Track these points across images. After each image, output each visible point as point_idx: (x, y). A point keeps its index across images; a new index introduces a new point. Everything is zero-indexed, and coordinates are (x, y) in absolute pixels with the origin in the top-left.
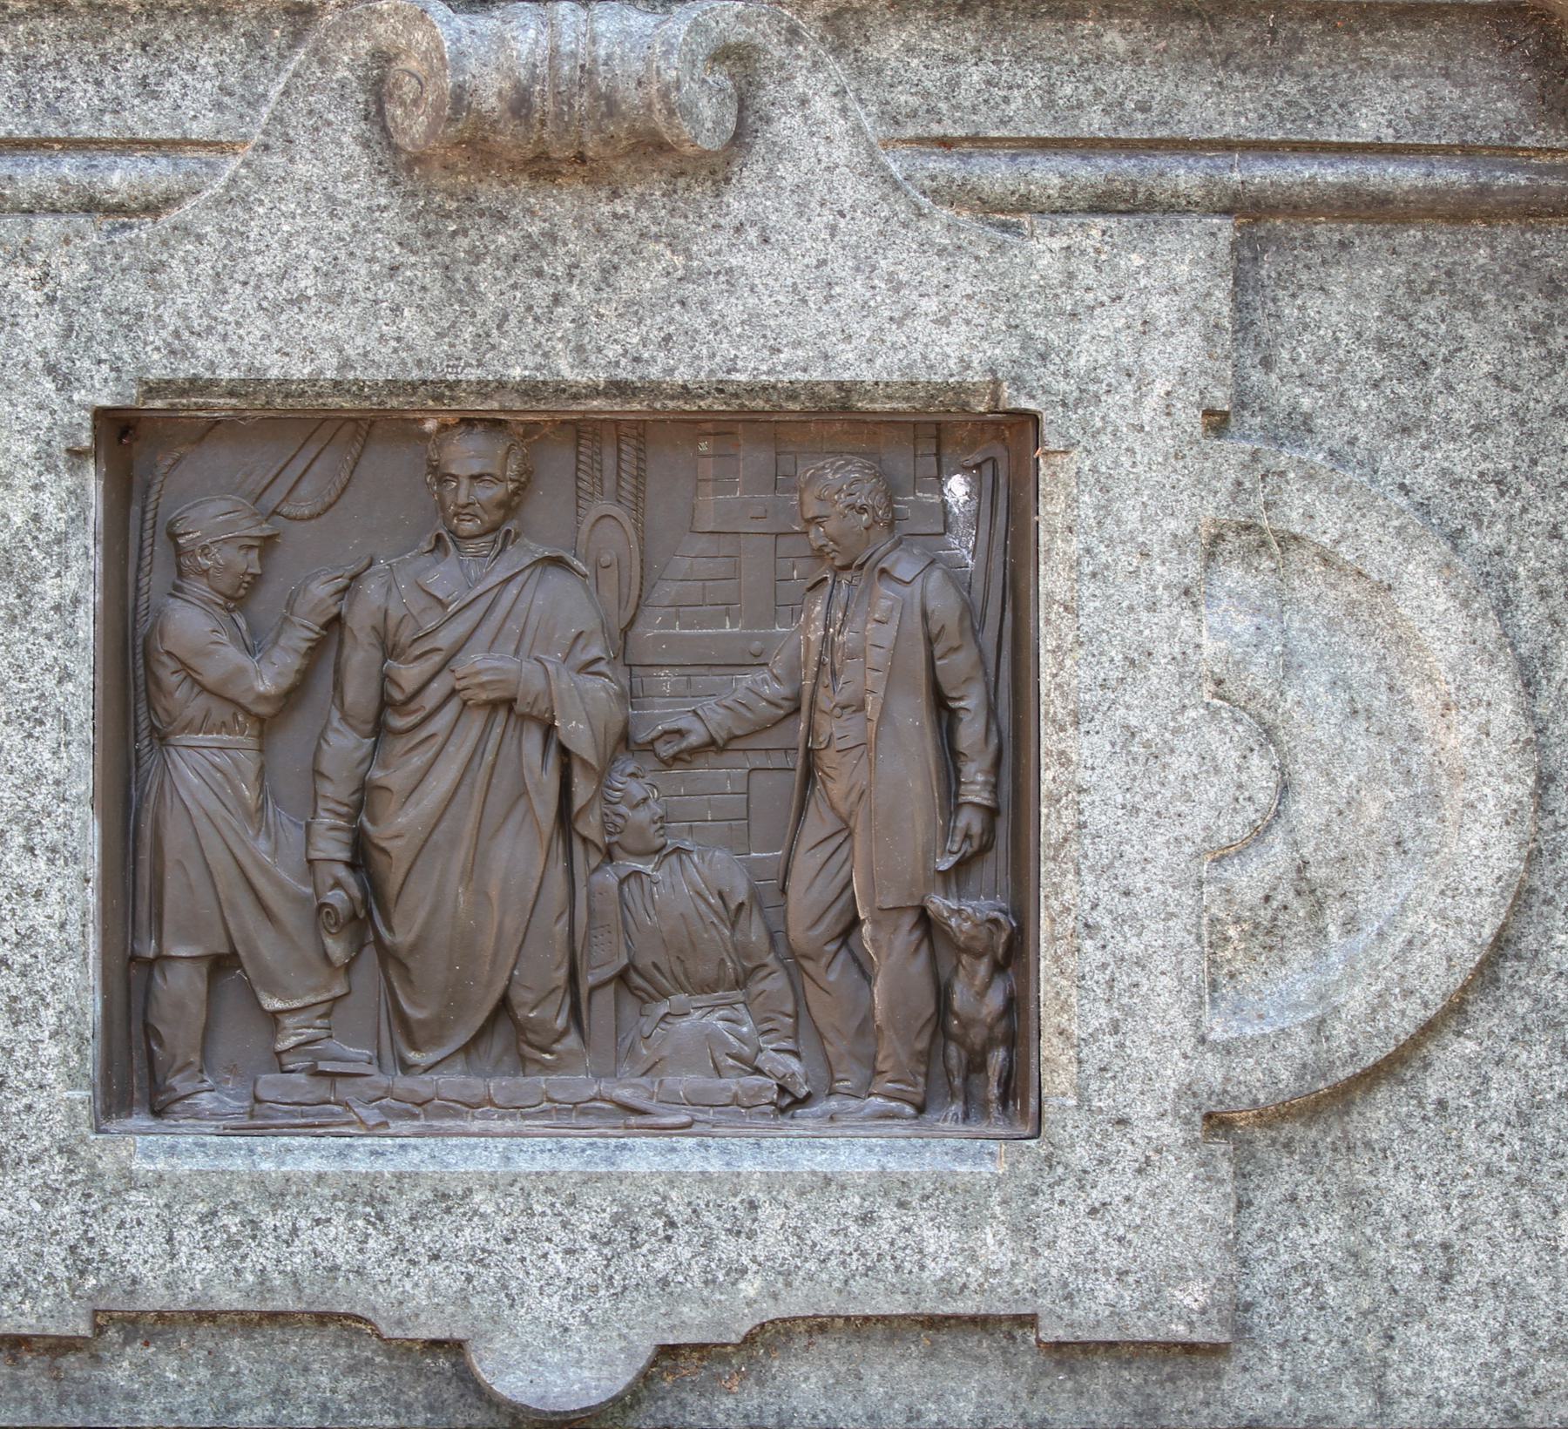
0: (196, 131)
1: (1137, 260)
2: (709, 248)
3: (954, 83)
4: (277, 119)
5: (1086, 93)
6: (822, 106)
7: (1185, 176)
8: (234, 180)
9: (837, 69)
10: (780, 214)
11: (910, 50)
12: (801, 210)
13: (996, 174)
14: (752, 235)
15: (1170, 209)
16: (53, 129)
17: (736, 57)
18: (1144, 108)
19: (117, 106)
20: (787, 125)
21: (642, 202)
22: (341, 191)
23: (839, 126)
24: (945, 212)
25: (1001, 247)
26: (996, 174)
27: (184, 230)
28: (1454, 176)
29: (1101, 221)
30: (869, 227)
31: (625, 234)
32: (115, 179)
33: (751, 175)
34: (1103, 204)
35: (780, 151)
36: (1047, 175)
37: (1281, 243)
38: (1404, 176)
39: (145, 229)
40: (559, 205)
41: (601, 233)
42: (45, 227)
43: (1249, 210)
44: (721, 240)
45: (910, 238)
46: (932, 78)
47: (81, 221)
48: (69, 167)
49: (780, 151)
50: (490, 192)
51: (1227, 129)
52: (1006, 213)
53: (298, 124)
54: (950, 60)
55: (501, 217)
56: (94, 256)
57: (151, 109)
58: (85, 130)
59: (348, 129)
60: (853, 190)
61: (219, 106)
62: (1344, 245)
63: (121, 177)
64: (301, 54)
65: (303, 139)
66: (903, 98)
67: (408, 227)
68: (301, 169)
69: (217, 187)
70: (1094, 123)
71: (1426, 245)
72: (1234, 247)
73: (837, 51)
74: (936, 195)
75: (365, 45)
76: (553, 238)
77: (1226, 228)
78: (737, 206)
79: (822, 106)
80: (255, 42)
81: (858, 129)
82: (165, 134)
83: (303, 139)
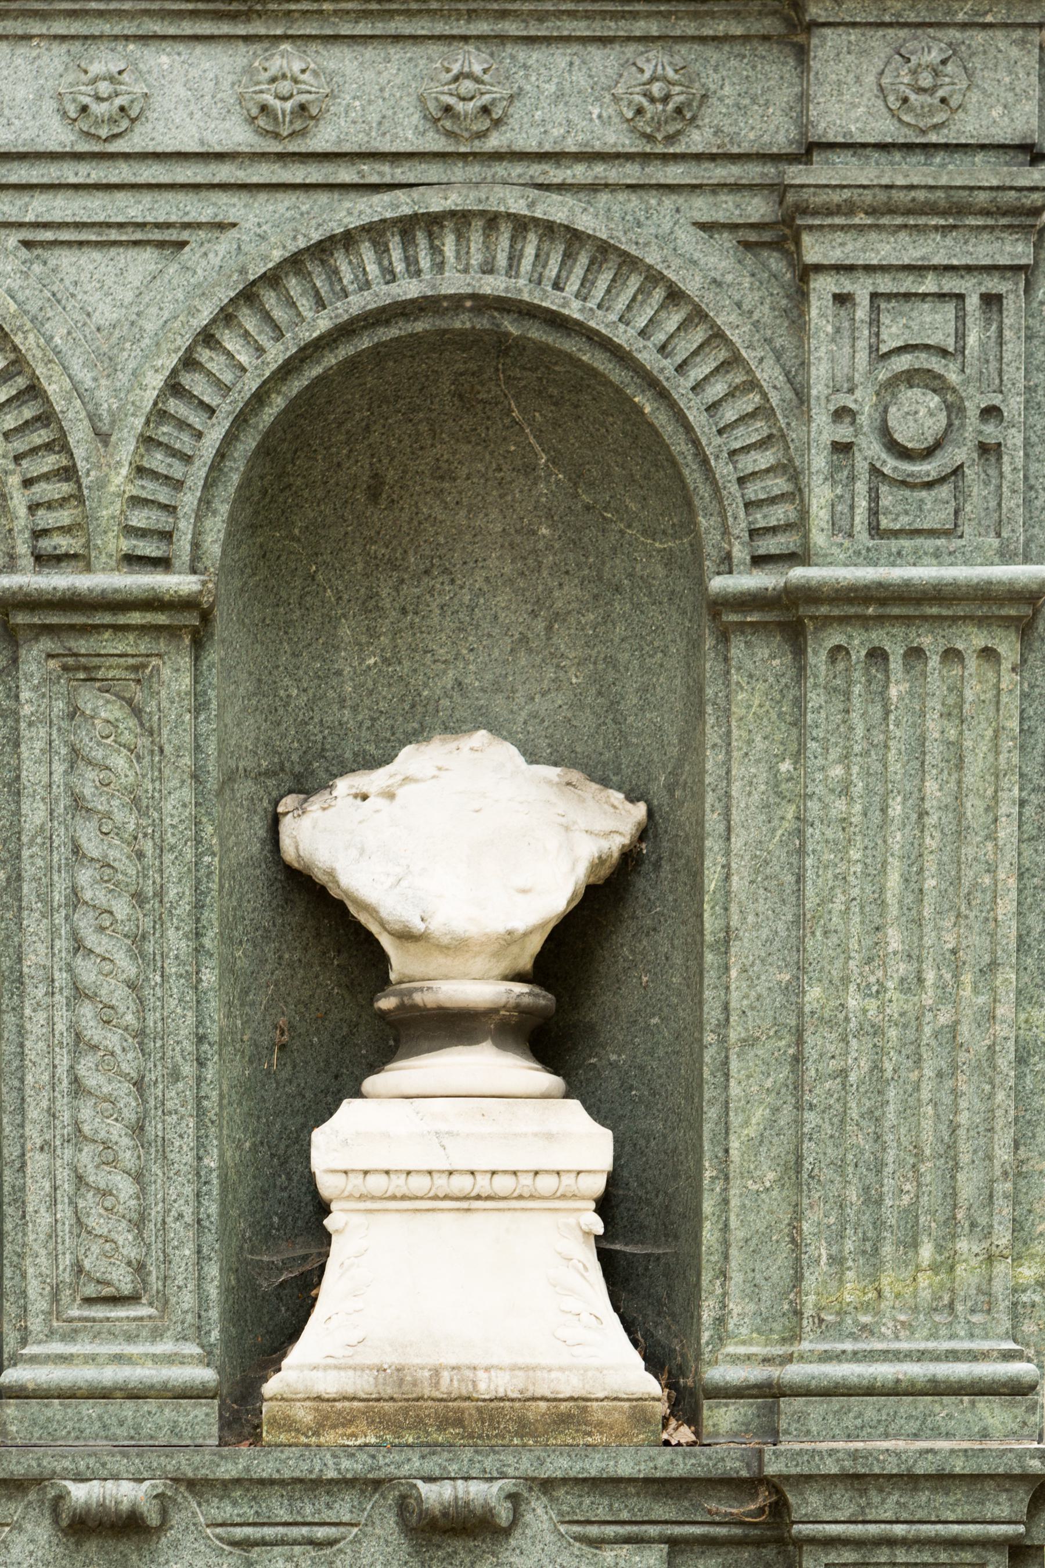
0: (345, 1519)
1: (638, 1559)
2: (506, 1556)
3: (581, 1503)
4: (369, 1516)
5: (622, 1506)
6: (540, 1511)
7: (653, 1531)
8: (356, 1535)
9: (544, 1499)
10: (526, 1544)
11: (567, 1493)
12: (533, 1544)
13: (593, 1531)
14: (518, 1551)
15: (648, 1542)
16: (300, 1519)
17: (513, 1498)
18: (640, 1510)
19: (319, 1512)
20: (529, 1517)
21: (484, 1541)
22: (390, 1539)
23: (545, 1517)
24: (577, 1544)
25: (595, 1555)
26: (593, 1531)
27: (340, 1551)
28: (737, 1531)
29: (626, 1546)
30: (554, 1549)
31: (478, 1552)
32: (319, 1535)
33: (518, 1533)
34: (628, 1540)
35: (527, 1525)
36: (610, 1531)
37: (682, 1552)
38: (722, 1531)
39: (328, 1551)
40: (458, 1544)
41: (471, 1551)
42: (297, 1549)
43: (674, 1543)
44: (508, 1553)
45: (567, 1552)
46: (574, 1502)
47: (309, 1547)
48: (305, 1530)
49: (527, 1525)
50: (436, 1539)
51: (667, 1517)
52: (597, 1543)
53: (376, 1518)
54: (580, 1496)
55: (439, 1547)
56: (312, 1559)
57: (330, 1513)
58: (309, 1519)
59: (391, 1520)
60: (549, 1538)
61: (351, 1512)
62: (703, 1553)
63: (321, 1533)
64: (377, 1496)
65: (378, 1522)
66: (565, 1508)
67: (410, 1550)
68: (377, 1531)
69: (351, 1537)
70: (625, 1516)
71: (729, 1552)
72: (669, 1553)
73: (545, 1494)
74: (575, 1539)
75: (397, 1493)
76: (455, 1552)
77: (665, 1547)
78: (513, 1542)
79: (540, 1511)
80: (363, 1491)
81: (551, 1518)
82: (334, 1520)
83: (378, 1522)
